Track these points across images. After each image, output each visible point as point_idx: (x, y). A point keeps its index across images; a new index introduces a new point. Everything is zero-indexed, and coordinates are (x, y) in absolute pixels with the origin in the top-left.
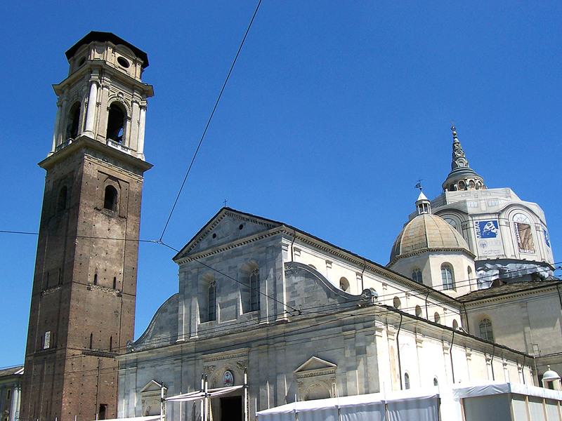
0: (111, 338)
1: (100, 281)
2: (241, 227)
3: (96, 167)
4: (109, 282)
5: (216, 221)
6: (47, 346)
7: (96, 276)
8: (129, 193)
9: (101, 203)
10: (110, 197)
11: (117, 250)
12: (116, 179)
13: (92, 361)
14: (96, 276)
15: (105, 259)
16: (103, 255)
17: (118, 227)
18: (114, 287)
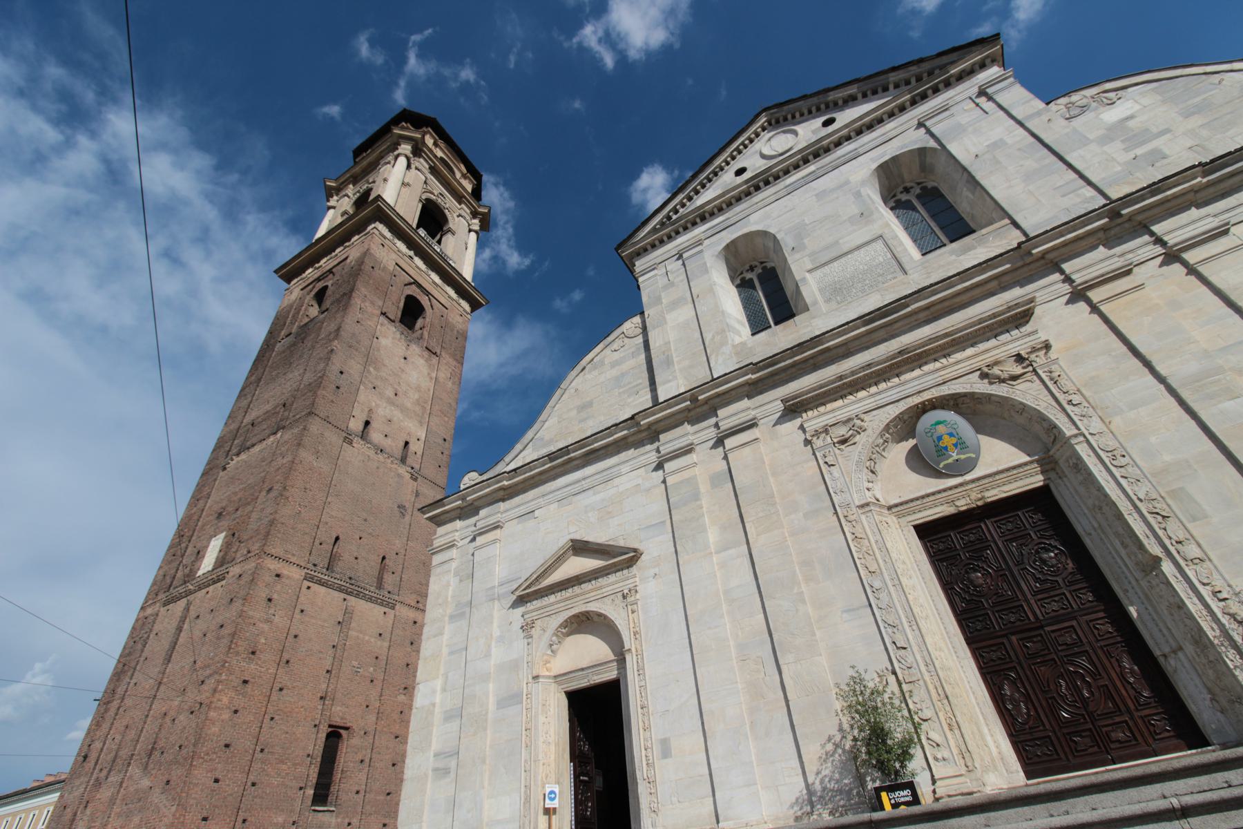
0: (384, 558)
1: (375, 435)
2: (827, 123)
3: (394, 256)
4: (395, 446)
5: (743, 144)
6: (207, 563)
7: (367, 423)
8: (445, 326)
9: (396, 311)
10: (411, 312)
11: (416, 396)
12: (427, 293)
13: (326, 600)
14: (367, 423)
15: (391, 402)
16: (389, 393)
17: (421, 362)
18: (403, 460)
